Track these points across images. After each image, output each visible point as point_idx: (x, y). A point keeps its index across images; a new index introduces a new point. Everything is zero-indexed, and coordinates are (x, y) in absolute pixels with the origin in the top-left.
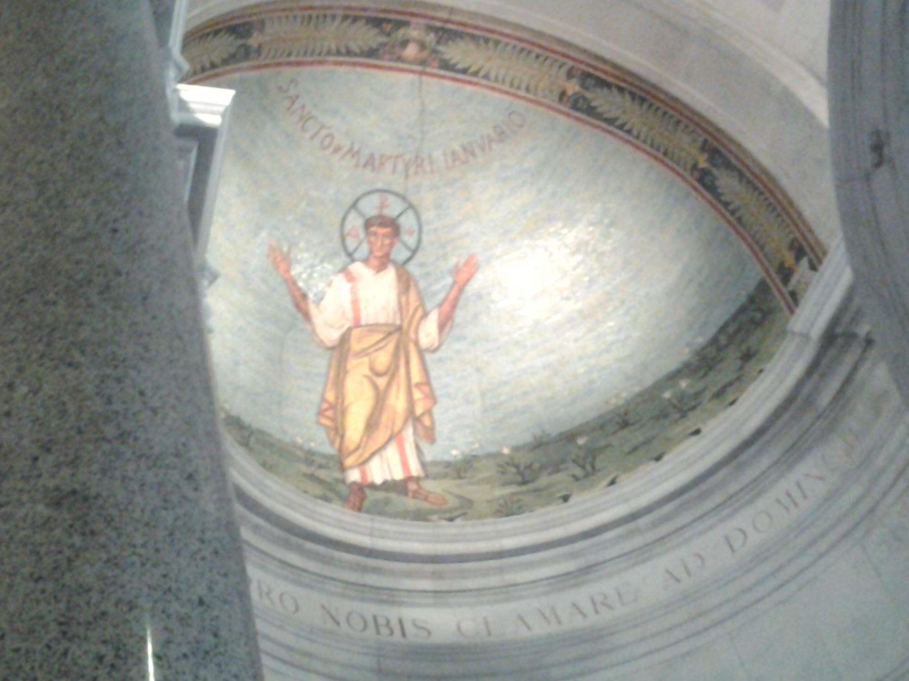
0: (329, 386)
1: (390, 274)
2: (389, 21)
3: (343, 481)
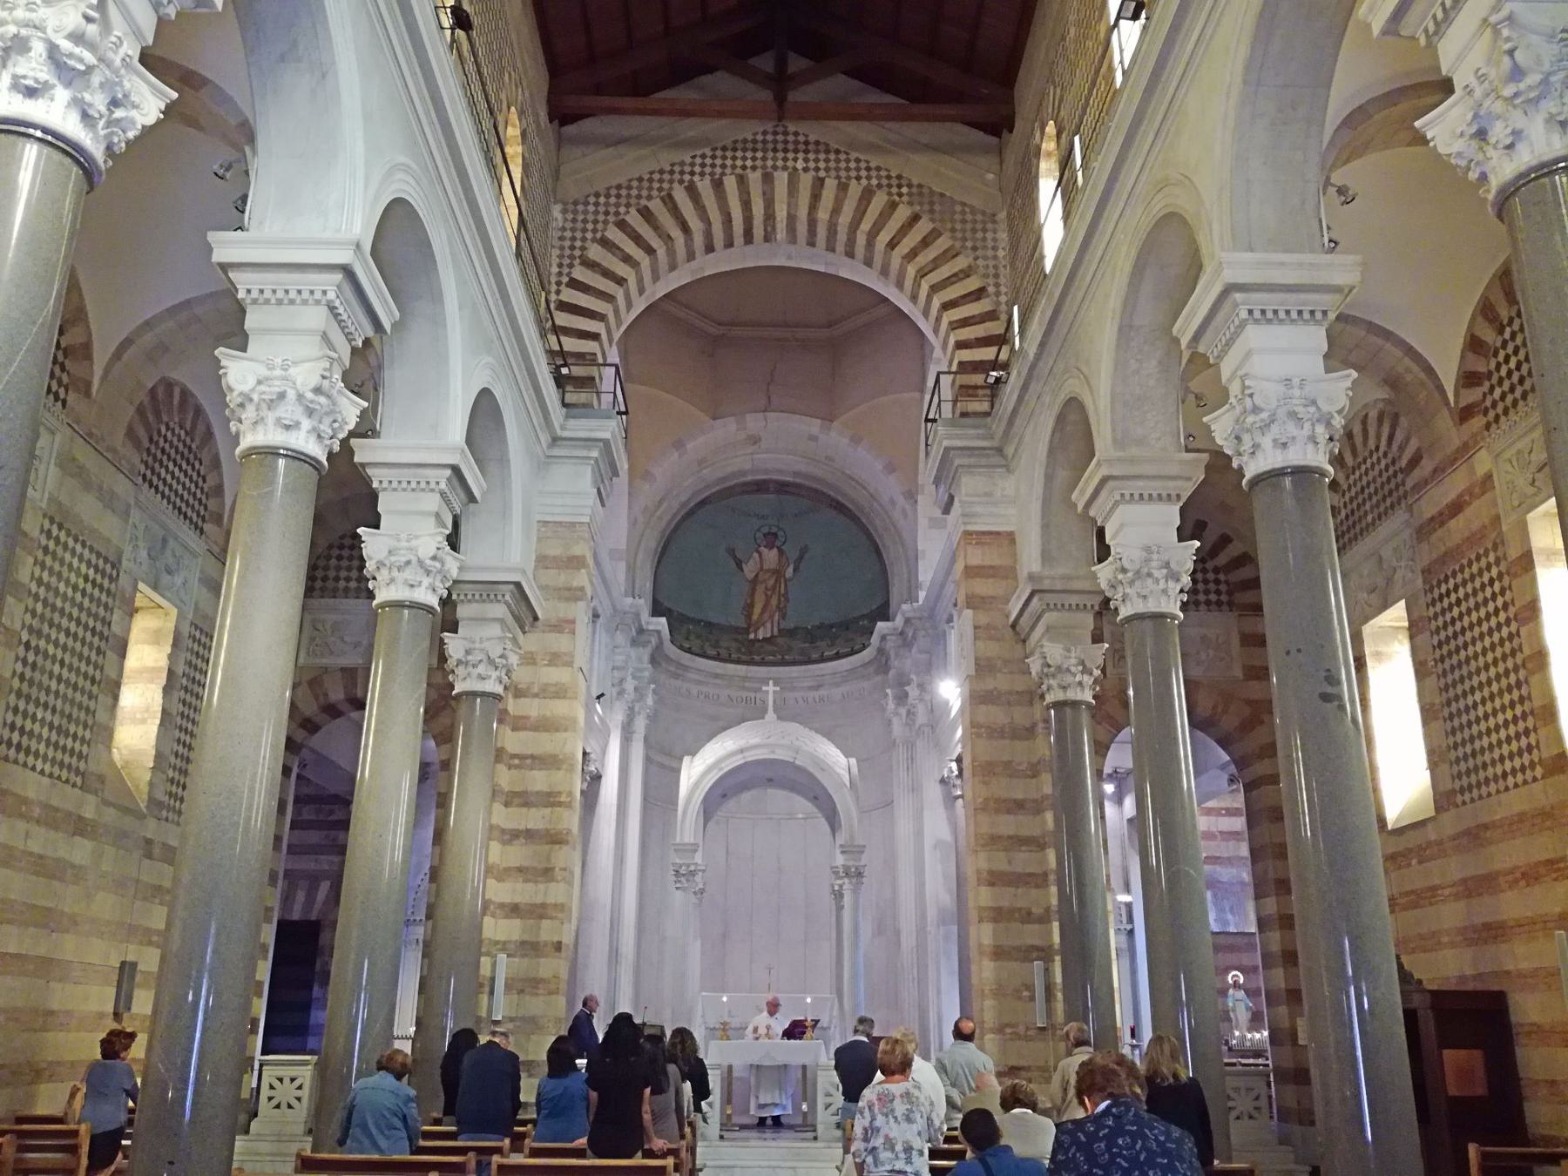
1: (775, 550)
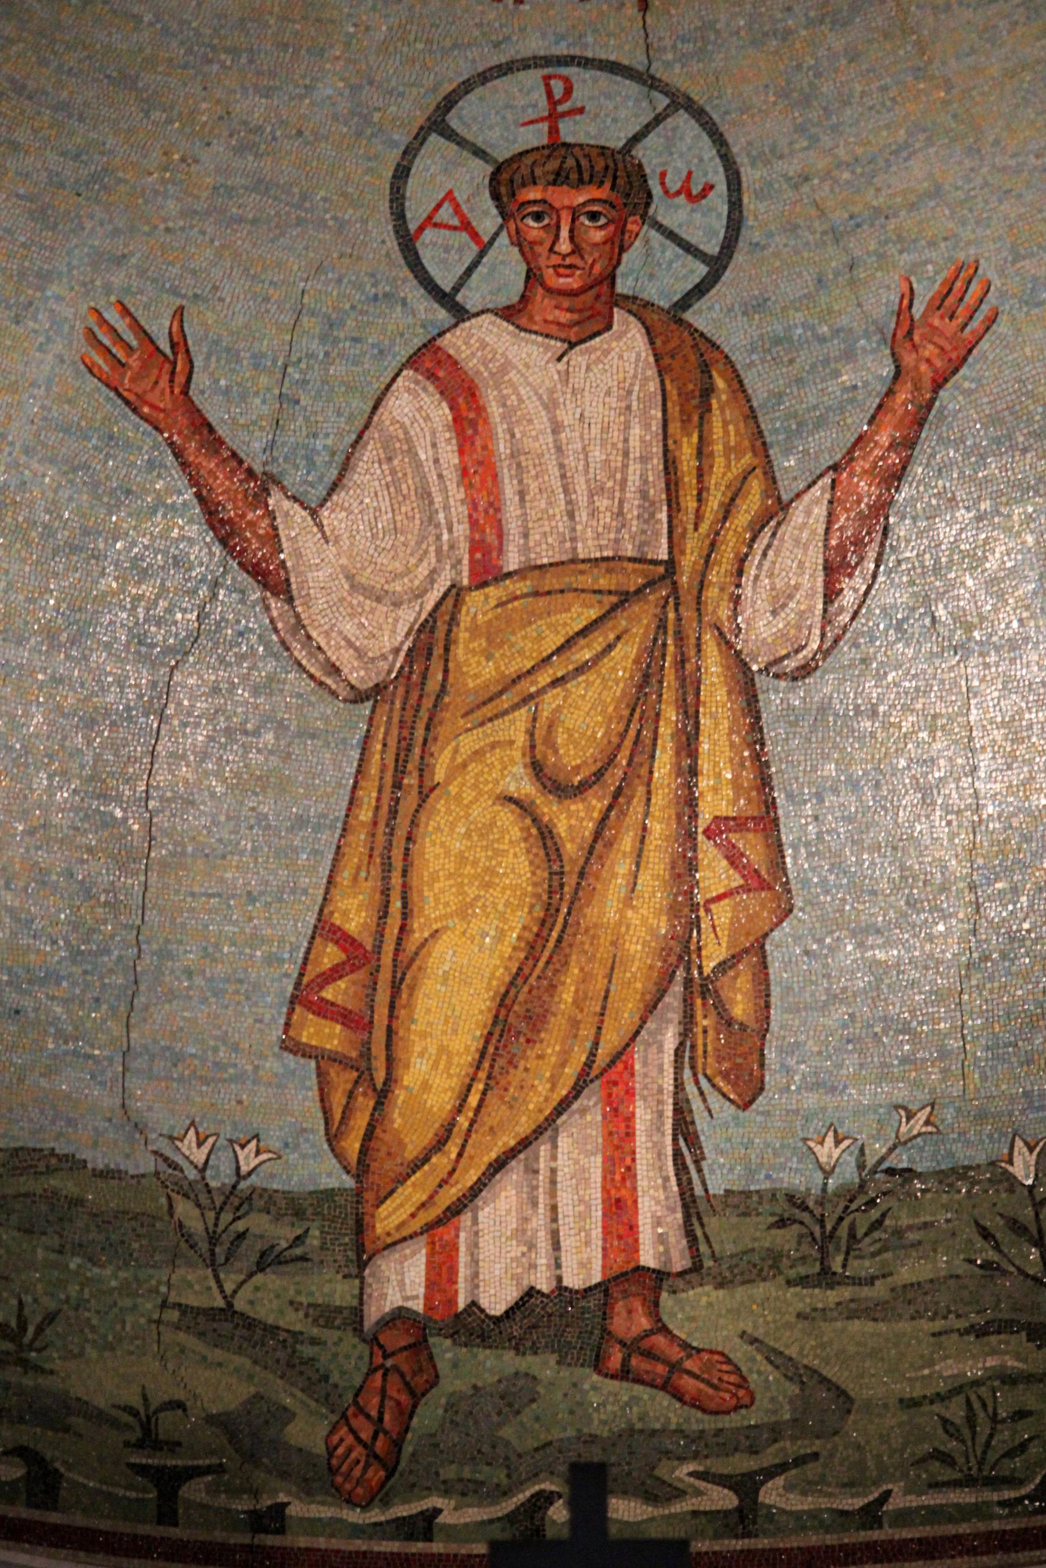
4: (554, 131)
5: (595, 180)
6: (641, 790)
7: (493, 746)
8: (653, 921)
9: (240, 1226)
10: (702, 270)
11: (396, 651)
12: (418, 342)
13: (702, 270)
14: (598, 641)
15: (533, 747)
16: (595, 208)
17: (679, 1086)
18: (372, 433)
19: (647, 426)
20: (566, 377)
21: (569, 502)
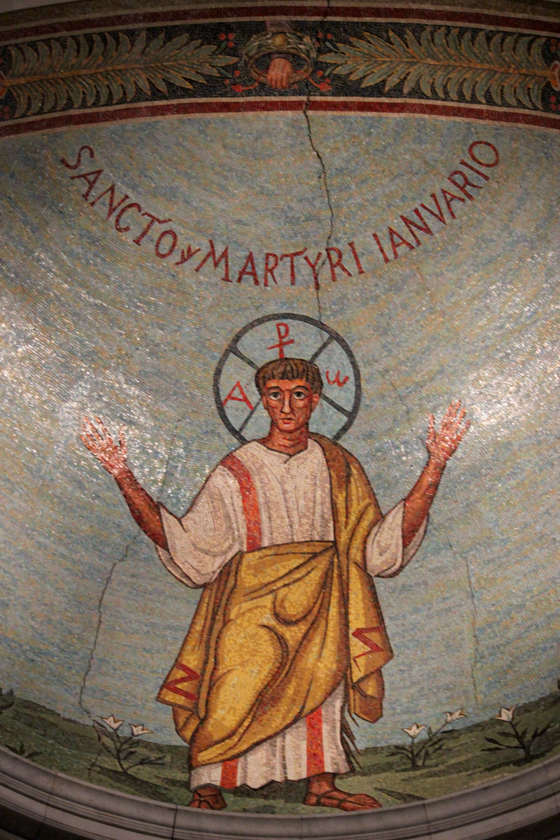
0: (192, 642)
2: (229, 28)
3: (187, 785)
4: (281, 351)
5: (299, 376)
6: (324, 621)
7: (257, 607)
8: (329, 665)
9: (133, 750)
10: (345, 419)
11: (214, 572)
12: (225, 453)
13: (345, 419)
14: (303, 571)
15: (275, 607)
16: (299, 390)
17: (343, 718)
18: (205, 491)
19: (323, 491)
20: (288, 470)
21: (290, 521)
